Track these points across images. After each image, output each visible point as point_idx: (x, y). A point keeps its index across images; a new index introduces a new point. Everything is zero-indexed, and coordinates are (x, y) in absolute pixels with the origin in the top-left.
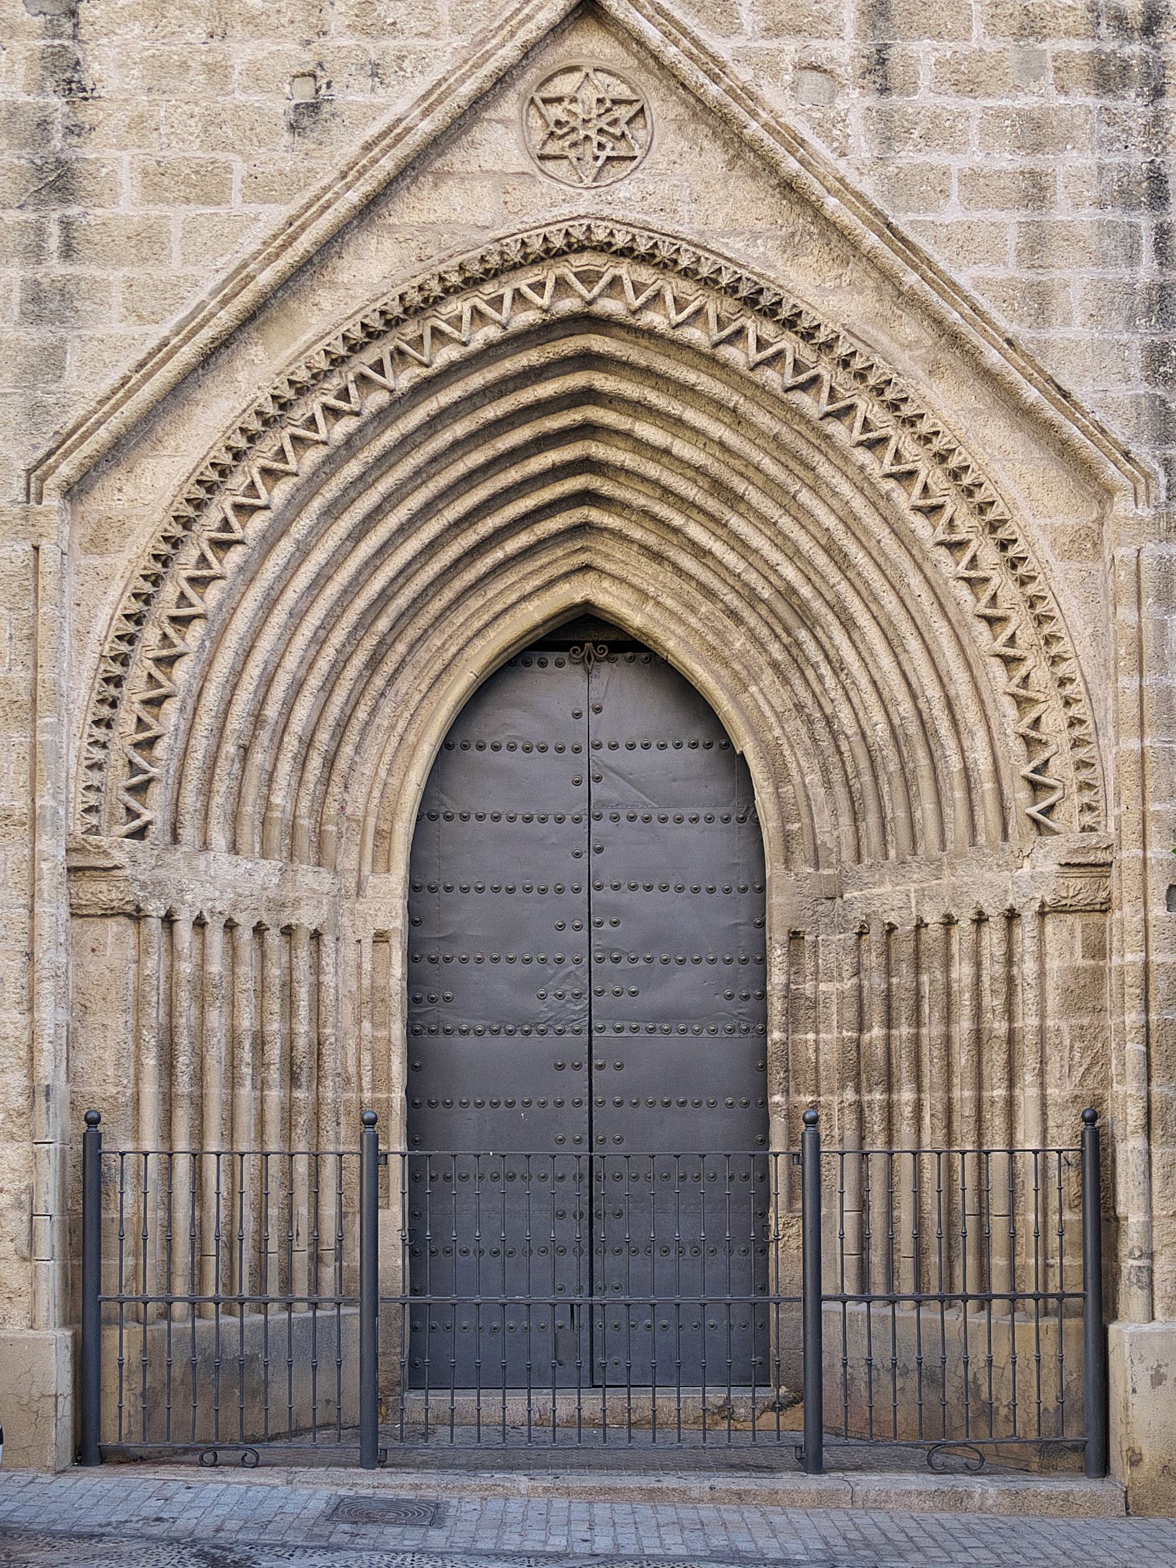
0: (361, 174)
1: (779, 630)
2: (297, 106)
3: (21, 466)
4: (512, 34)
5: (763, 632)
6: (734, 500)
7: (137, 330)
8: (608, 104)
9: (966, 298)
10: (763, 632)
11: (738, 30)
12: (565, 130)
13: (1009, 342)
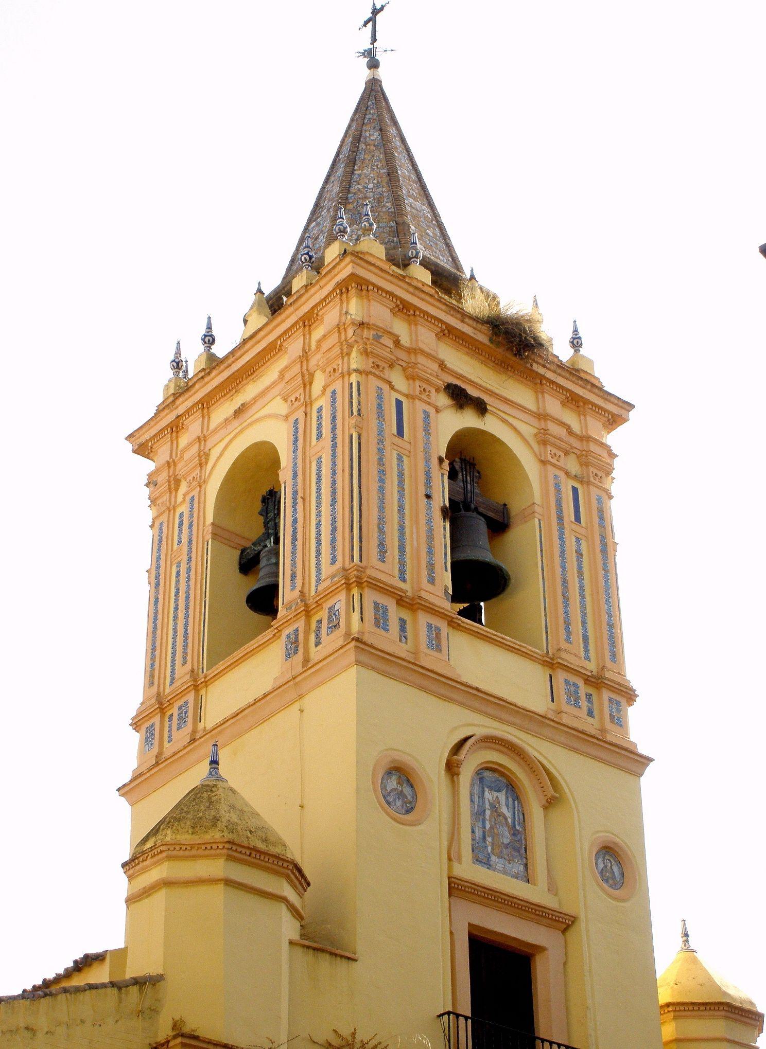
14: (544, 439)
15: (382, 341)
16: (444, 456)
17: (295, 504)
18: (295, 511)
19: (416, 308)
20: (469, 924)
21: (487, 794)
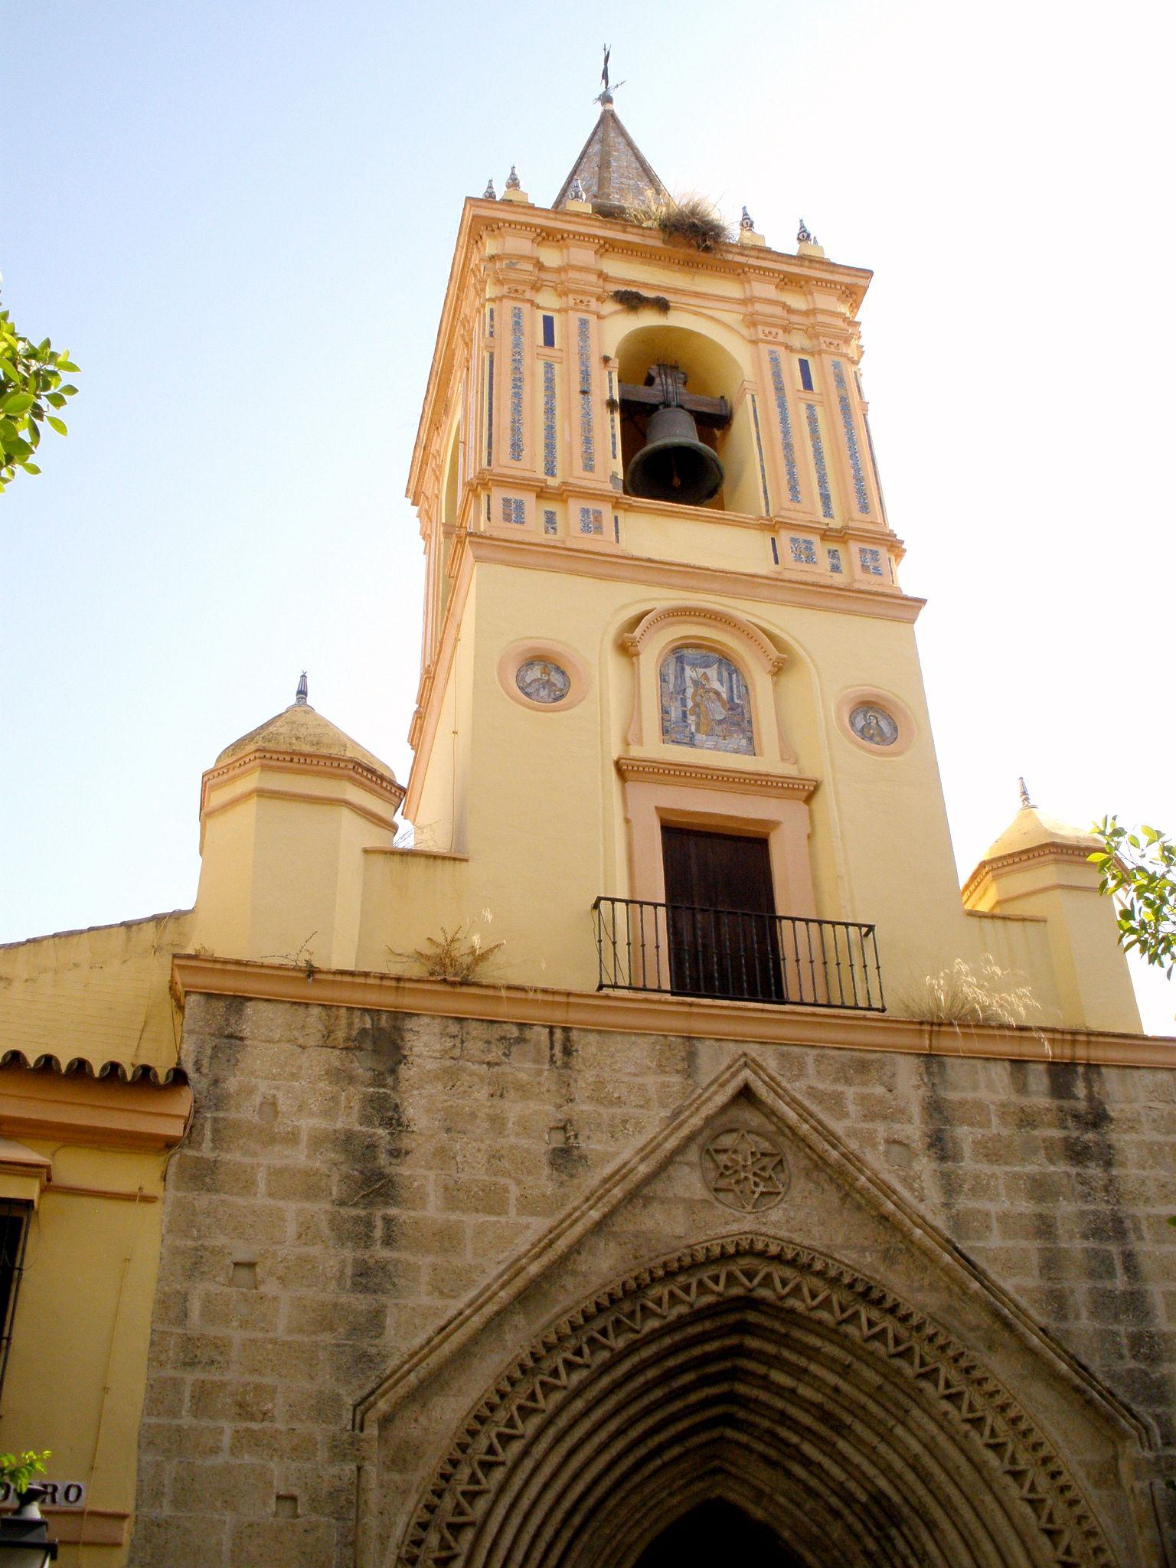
0: (599, 1199)
1: (870, 1525)
2: (554, 1149)
3: (349, 1402)
4: (697, 1109)
5: (859, 1527)
6: (839, 1428)
7: (439, 1303)
8: (759, 1156)
9: (1010, 1300)
10: (859, 1527)
11: (845, 1115)
12: (731, 1172)
13: (1042, 1330)
14: (752, 322)
15: (518, 266)
16: (611, 353)
19: (562, 231)
20: (657, 808)
21: (689, 672)
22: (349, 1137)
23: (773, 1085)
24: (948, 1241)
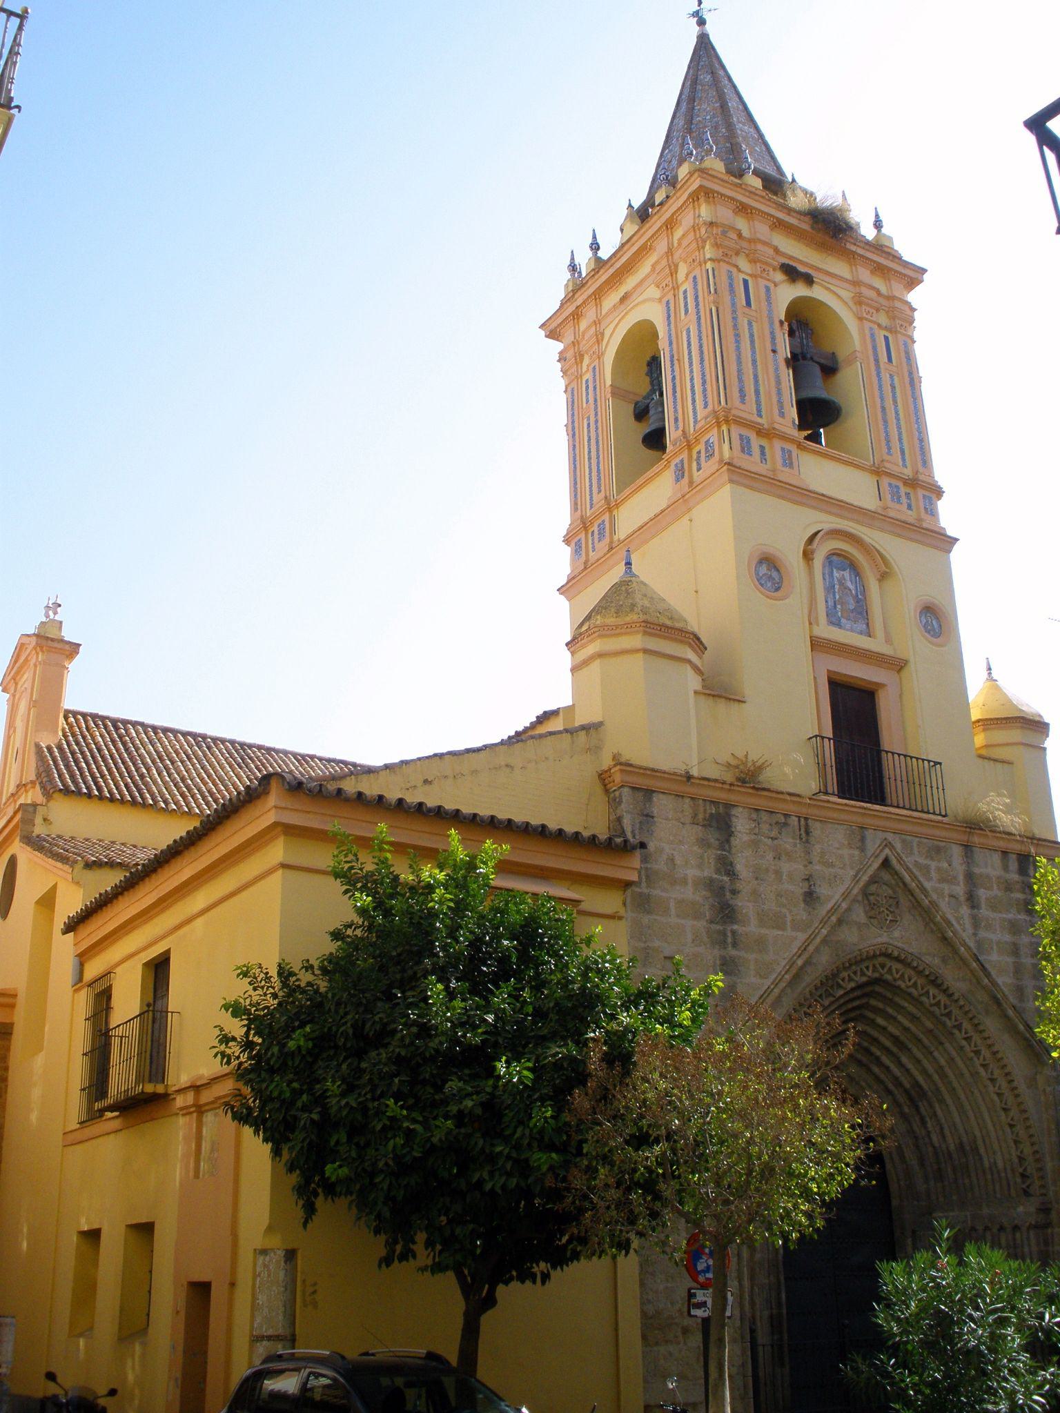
14: (859, 301)
15: (728, 235)
16: (783, 318)
17: (672, 365)
18: (673, 371)
19: (752, 208)
21: (836, 574)
22: (712, 880)
23: (899, 859)
24: (975, 955)
